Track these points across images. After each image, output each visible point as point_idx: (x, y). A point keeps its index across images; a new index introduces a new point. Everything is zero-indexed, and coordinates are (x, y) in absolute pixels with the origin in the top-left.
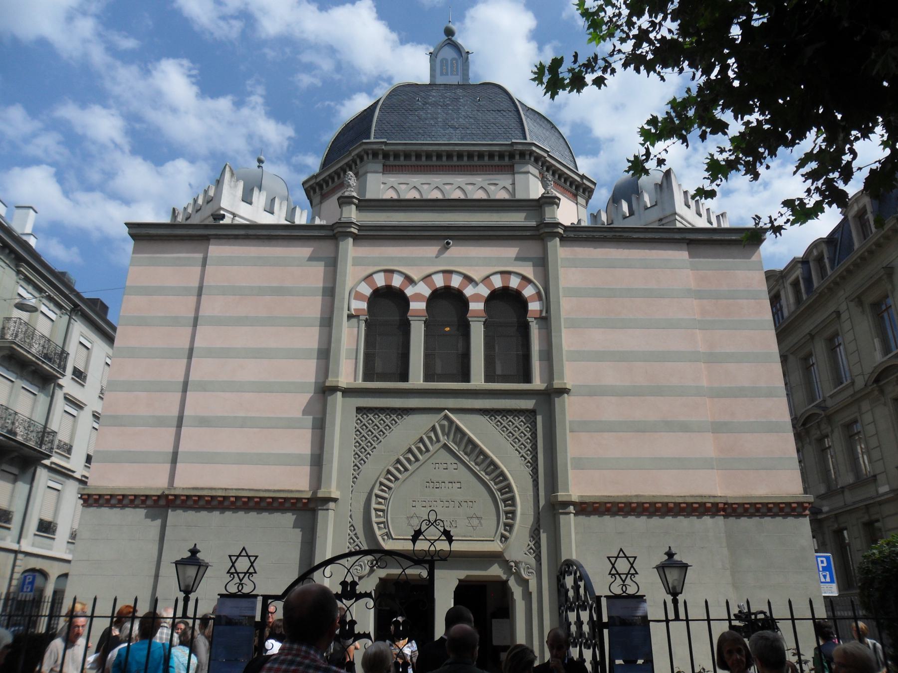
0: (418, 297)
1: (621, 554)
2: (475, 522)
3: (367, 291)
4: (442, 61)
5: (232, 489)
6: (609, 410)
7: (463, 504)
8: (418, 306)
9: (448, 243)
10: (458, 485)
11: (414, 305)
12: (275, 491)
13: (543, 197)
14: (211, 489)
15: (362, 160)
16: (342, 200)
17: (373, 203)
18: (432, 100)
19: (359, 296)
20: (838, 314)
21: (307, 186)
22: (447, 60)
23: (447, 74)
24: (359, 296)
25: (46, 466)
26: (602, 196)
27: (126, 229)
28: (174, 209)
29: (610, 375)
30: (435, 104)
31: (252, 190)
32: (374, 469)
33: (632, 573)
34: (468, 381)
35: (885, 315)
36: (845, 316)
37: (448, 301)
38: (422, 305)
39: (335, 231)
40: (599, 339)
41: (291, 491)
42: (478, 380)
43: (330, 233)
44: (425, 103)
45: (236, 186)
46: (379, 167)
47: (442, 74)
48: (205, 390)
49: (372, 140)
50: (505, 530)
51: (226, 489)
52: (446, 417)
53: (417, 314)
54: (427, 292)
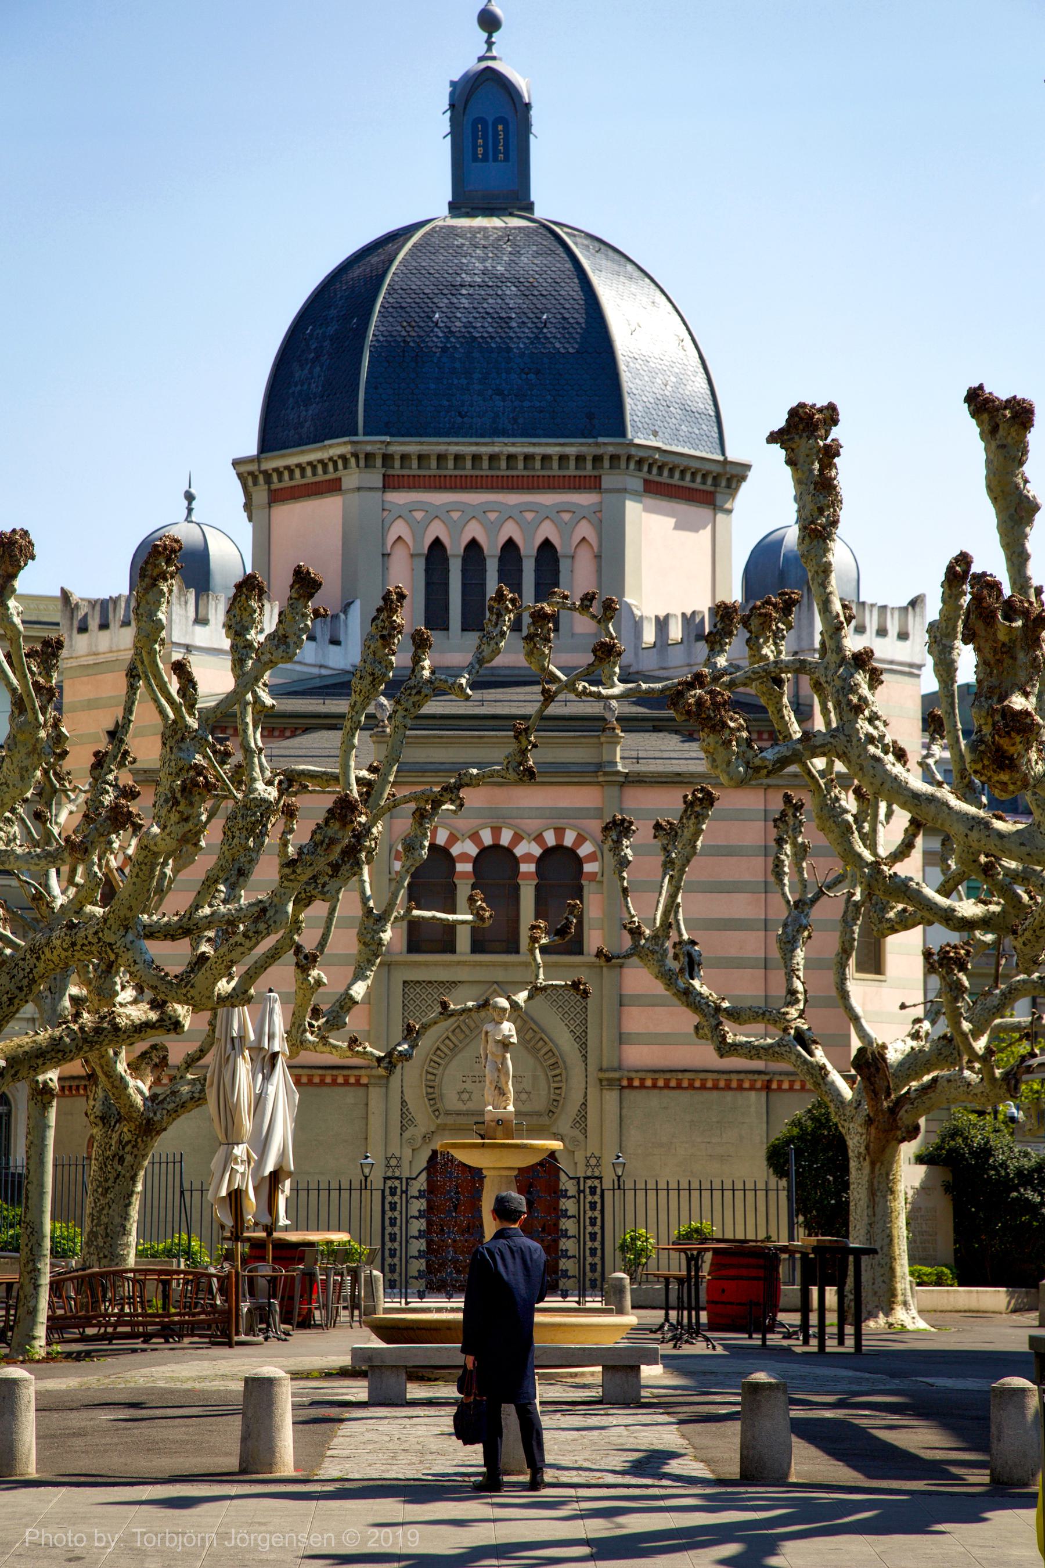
0: (464, 857)
11: (460, 867)
33: (598, 1166)
38: (468, 867)
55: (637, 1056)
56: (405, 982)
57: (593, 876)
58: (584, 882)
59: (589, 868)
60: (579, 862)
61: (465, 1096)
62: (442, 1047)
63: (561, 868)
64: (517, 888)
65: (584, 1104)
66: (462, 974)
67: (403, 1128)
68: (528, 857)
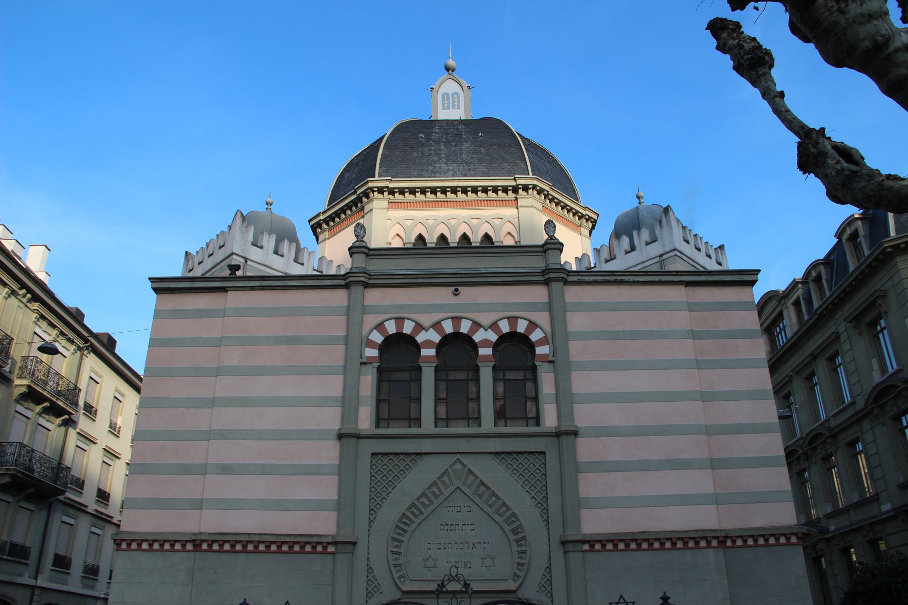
0: (428, 344)
1: (622, 600)
2: (488, 562)
3: (378, 338)
4: (443, 95)
5: (255, 534)
6: (616, 449)
7: (478, 546)
8: (428, 352)
9: (456, 290)
10: (472, 527)
12: (295, 536)
13: (546, 243)
14: (236, 534)
15: (367, 197)
16: (354, 250)
17: (383, 252)
18: (435, 136)
19: (370, 344)
20: (836, 337)
21: (312, 223)
22: (448, 94)
23: (448, 108)
24: (370, 344)
25: (61, 501)
26: (605, 229)
27: (149, 284)
28: (186, 253)
29: (616, 415)
30: (438, 141)
31: (262, 233)
32: (390, 512)
34: (480, 426)
35: (881, 335)
36: (843, 337)
37: (457, 345)
38: (432, 352)
39: (347, 281)
40: (606, 382)
41: (311, 536)
42: (488, 423)
43: (342, 282)
44: (428, 140)
45: (247, 231)
46: (385, 204)
47: (443, 108)
48: (226, 439)
49: (377, 178)
50: (519, 570)
51: (249, 534)
52: (459, 460)
53: (428, 359)
54: (436, 338)
55: (594, 523)
56: (373, 454)
57: (544, 359)
58: (537, 363)
59: (541, 350)
60: (531, 346)
61: (430, 563)
62: (408, 514)
63: (515, 347)
64: (477, 369)
65: (549, 568)
66: (427, 446)
67: (369, 595)
68: (485, 343)
